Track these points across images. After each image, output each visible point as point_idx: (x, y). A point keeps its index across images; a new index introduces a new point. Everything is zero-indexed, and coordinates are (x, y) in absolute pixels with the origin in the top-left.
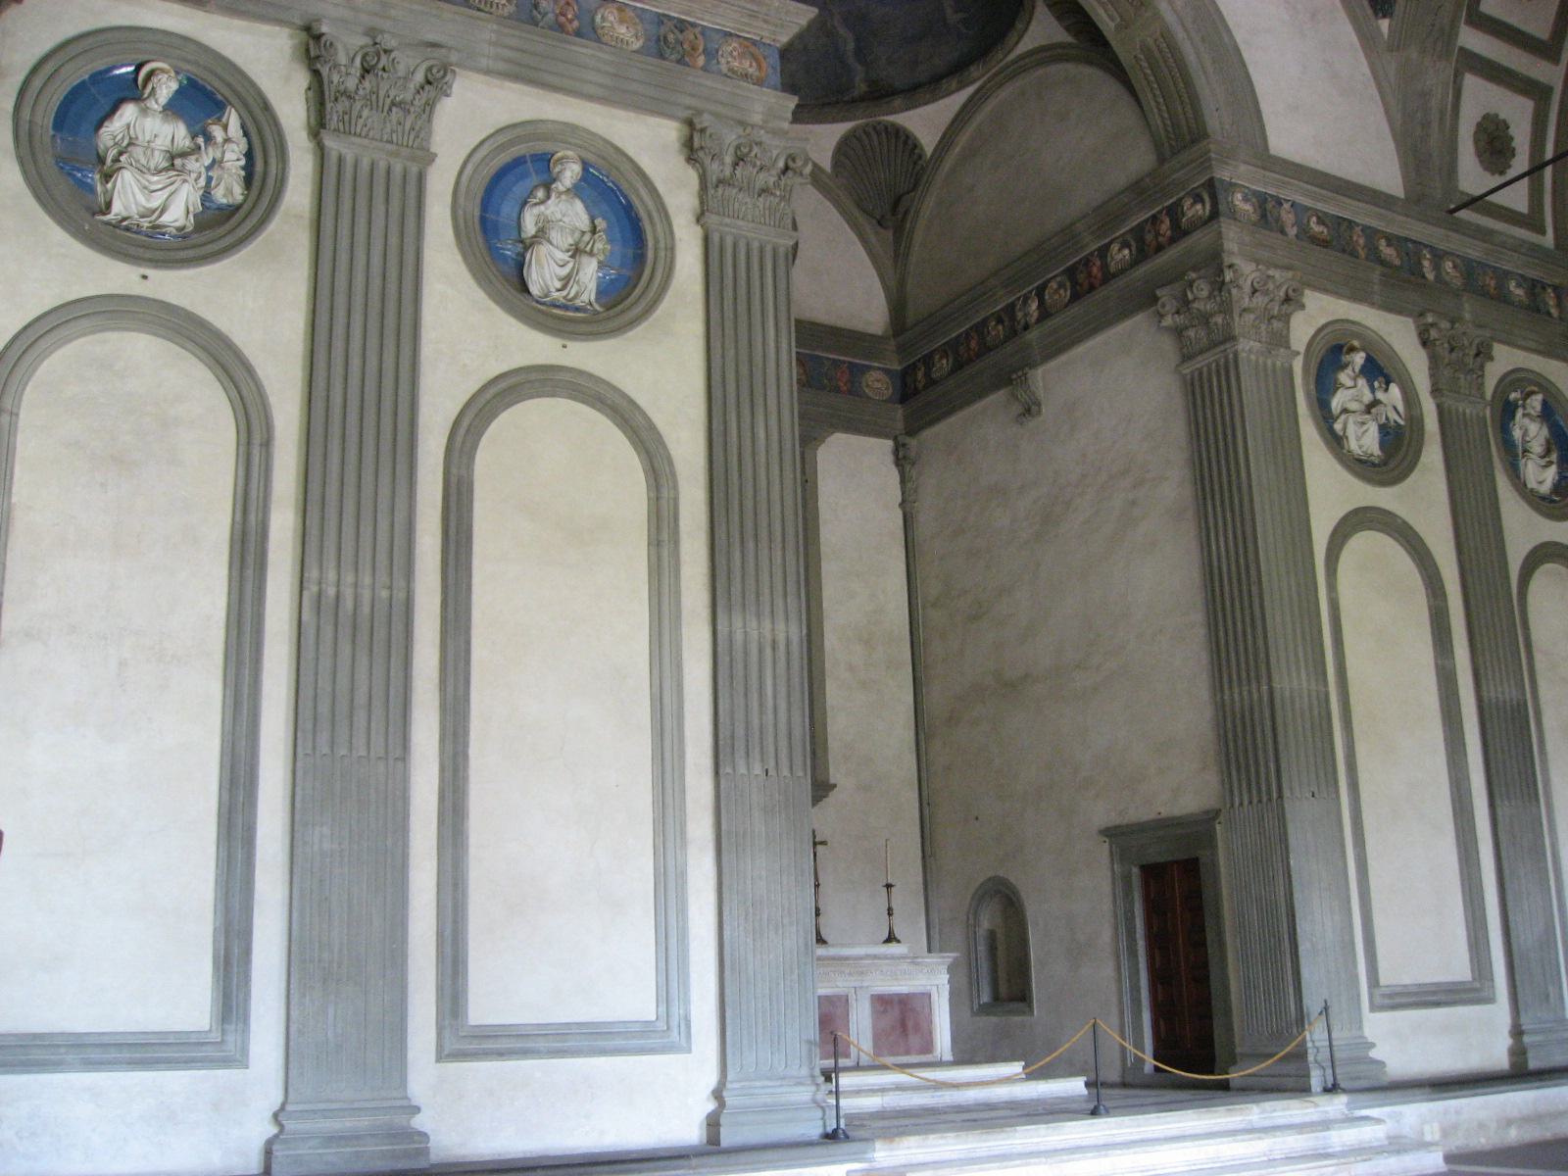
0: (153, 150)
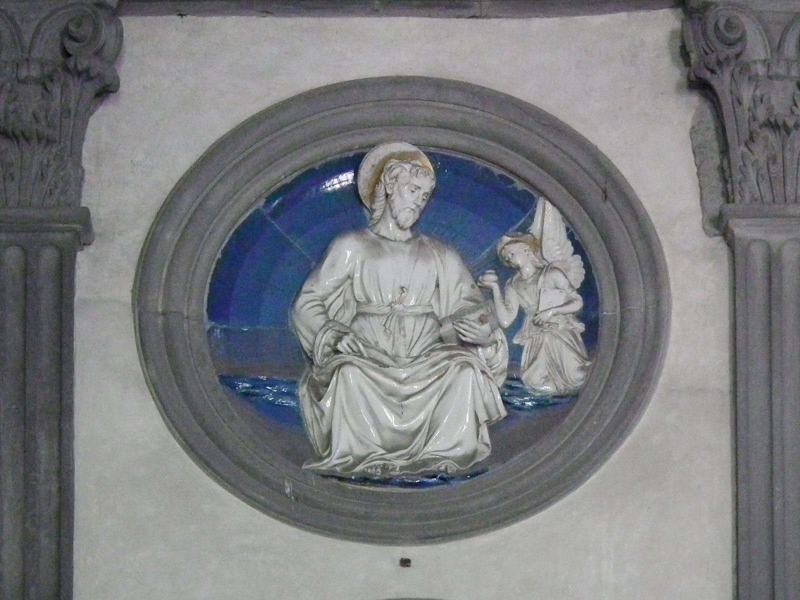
0: (400, 319)
